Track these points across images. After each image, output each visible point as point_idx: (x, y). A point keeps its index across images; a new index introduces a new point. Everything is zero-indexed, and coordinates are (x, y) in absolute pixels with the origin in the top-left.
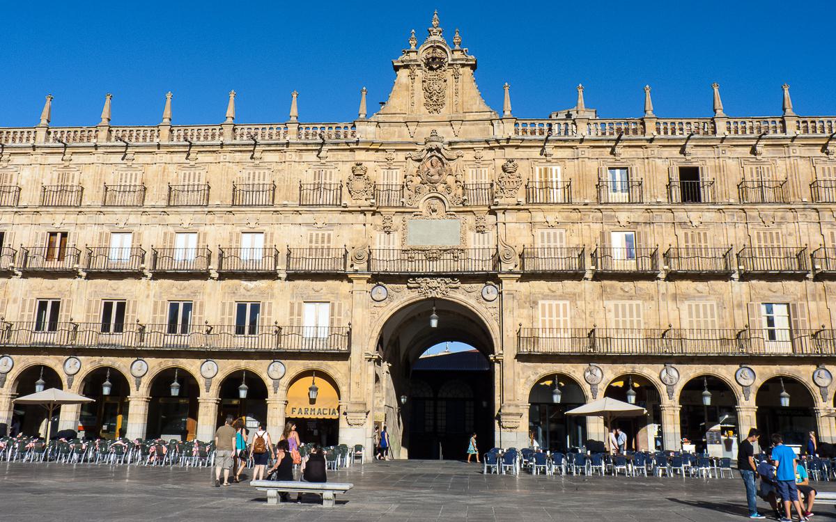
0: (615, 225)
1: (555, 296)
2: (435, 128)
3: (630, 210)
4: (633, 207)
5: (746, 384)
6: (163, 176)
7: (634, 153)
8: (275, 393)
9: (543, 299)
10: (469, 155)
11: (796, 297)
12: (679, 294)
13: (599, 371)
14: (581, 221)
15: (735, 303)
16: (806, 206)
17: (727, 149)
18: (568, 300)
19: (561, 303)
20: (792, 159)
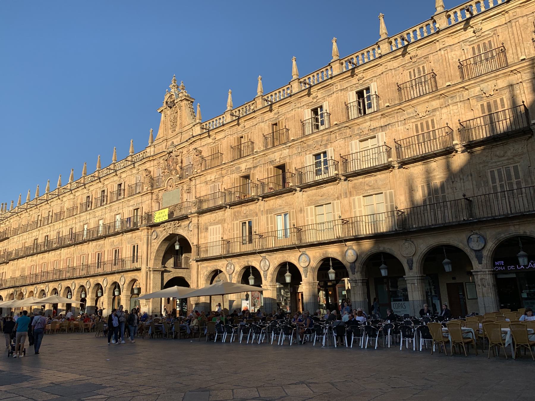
1: (215, 223)
2: (173, 141)
3: (246, 161)
5: (304, 266)
7: (251, 123)
9: (210, 226)
10: (185, 151)
12: (269, 210)
13: (232, 266)
14: (227, 174)
15: (299, 209)
16: (340, 127)
17: (296, 102)
19: (218, 226)
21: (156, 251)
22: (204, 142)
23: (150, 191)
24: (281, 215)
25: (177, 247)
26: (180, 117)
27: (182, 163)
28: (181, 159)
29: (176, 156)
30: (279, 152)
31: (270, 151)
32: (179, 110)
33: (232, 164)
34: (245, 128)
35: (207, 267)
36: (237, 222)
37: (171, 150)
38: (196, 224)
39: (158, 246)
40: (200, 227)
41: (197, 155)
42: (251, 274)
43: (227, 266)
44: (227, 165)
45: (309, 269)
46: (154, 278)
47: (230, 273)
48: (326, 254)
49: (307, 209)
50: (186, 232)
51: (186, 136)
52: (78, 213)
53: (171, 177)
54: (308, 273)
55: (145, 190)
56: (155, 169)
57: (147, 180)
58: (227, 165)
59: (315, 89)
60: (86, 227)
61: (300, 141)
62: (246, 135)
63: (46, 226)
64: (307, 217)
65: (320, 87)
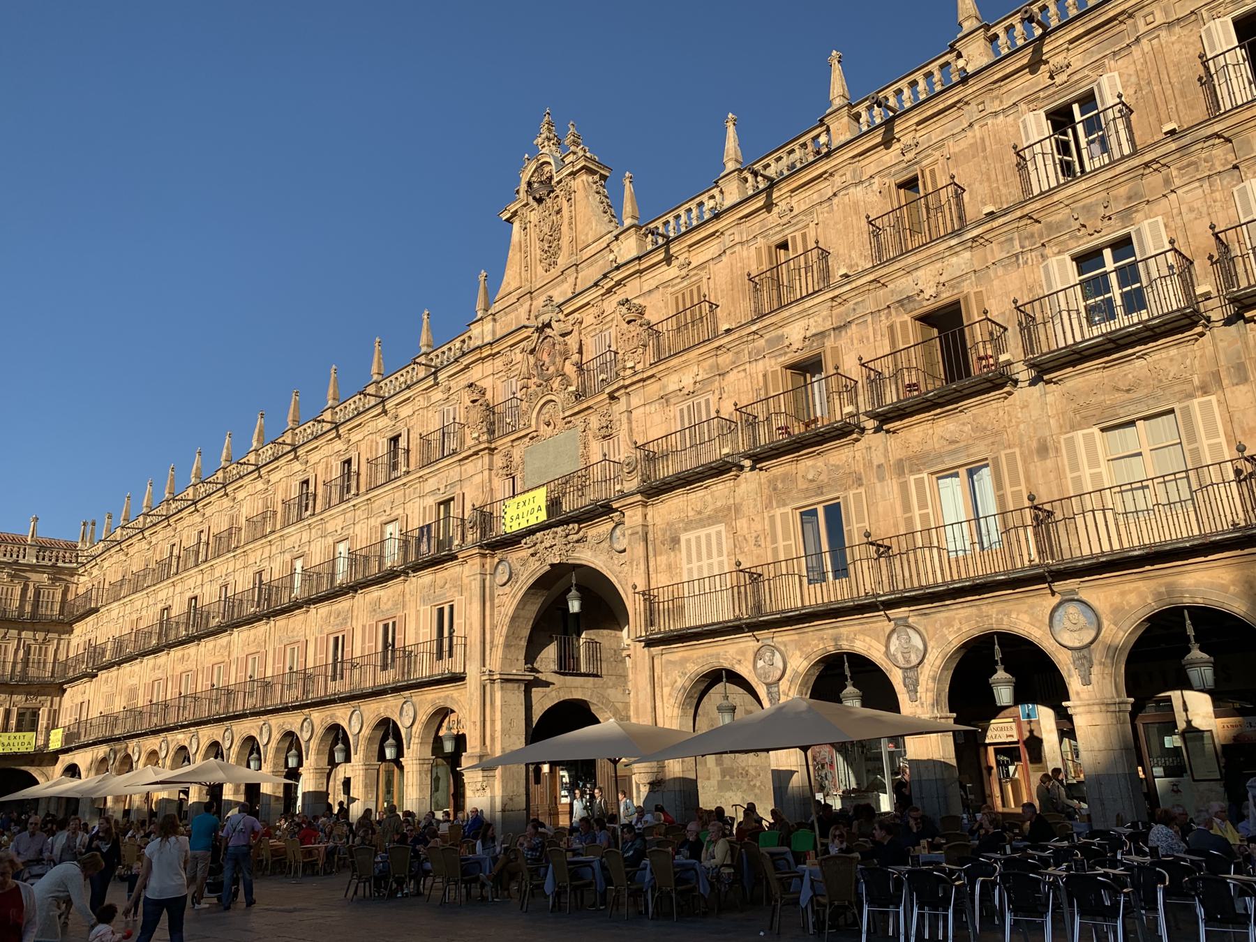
0: (786, 353)
1: (701, 520)
2: (549, 294)
3: (805, 314)
4: (807, 305)
5: (1077, 644)
6: (326, 474)
8: (409, 748)
9: (686, 530)
10: (589, 317)
11: (1188, 387)
12: (909, 458)
13: (777, 655)
14: (735, 365)
15: (1034, 445)
18: (721, 522)
19: (712, 530)
20: (1144, 41)
21: (508, 620)
22: (649, 281)
23: (486, 445)
24: (956, 475)
25: (575, 606)
26: (570, 224)
27: (580, 352)
28: (577, 339)
29: (563, 335)
30: (931, 267)
31: (897, 266)
32: (565, 205)
33: (754, 328)
34: (795, 212)
35: (684, 661)
36: (783, 510)
37: (546, 318)
38: (640, 529)
39: (513, 607)
40: (650, 536)
41: (629, 322)
42: (849, 682)
43: (757, 655)
44: (736, 335)
45: (1098, 654)
46: (505, 704)
47: (769, 681)
48: (1169, 593)
49: (1071, 443)
50: (604, 557)
51: (590, 273)
52: (278, 527)
53: (549, 397)
54: (1096, 670)
55: (469, 442)
56: (498, 382)
57: (476, 414)
58: (736, 335)
59: (1061, 41)
60: (298, 565)
61: (1018, 214)
62: (798, 235)
63: (192, 571)
64: (1075, 467)
65: (1081, 30)
